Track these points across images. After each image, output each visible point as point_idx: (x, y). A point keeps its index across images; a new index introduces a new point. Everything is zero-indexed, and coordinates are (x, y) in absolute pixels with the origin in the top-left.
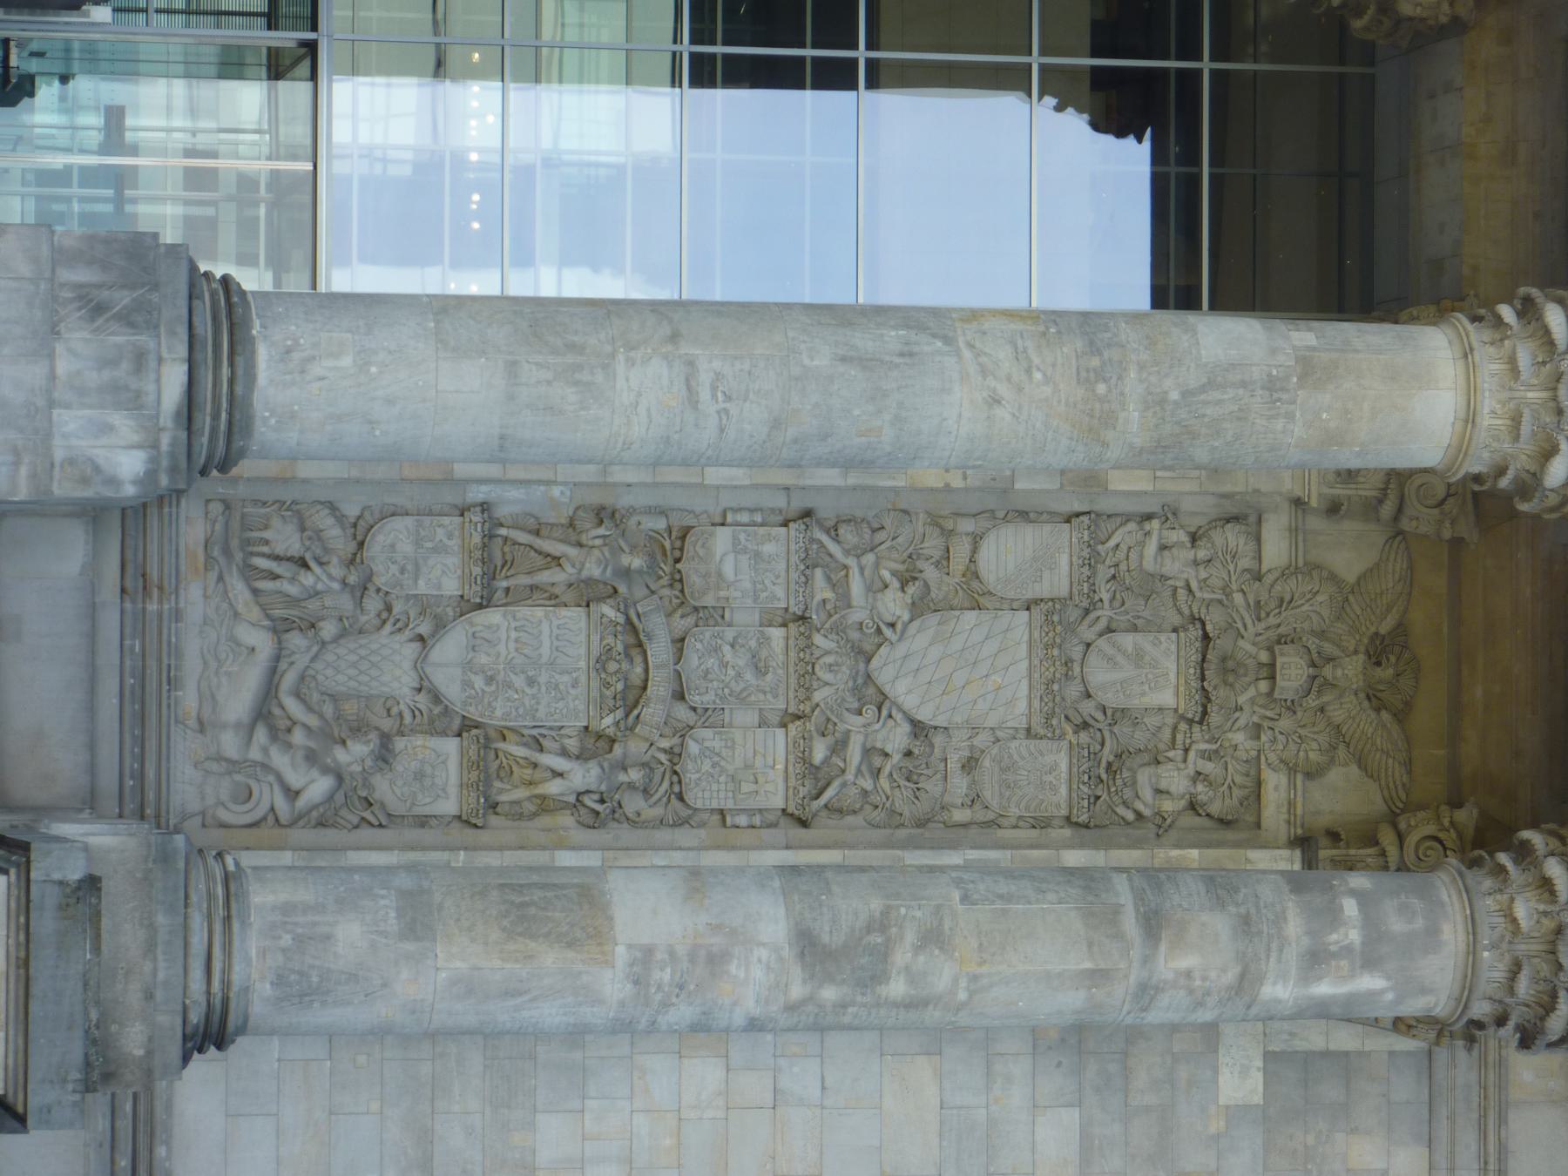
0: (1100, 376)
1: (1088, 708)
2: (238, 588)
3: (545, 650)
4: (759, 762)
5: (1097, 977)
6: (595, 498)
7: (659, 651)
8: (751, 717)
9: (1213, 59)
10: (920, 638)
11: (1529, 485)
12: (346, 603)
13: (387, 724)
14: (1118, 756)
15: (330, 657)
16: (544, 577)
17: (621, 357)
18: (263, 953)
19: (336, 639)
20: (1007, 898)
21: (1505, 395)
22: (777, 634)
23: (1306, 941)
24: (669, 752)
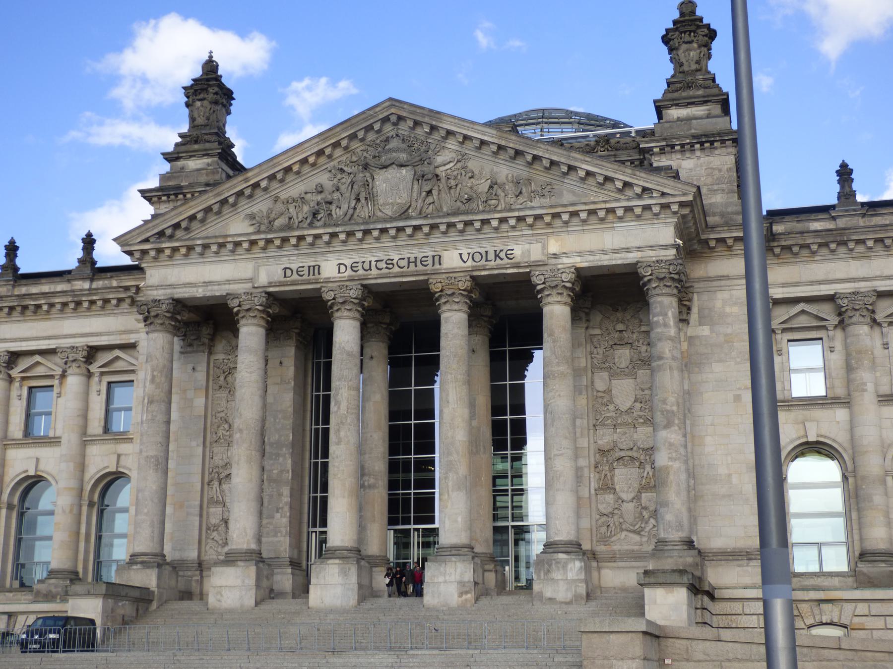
0: (554, 375)
1: (630, 367)
2: (614, 539)
3: (624, 477)
4: (644, 433)
5: (671, 368)
6: (592, 469)
7: (622, 454)
8: (635, 434)
9: (506, 347)
10: (617, 401)
11: (572, 289)
12: (616, 517)
13: (640, 507)
14: (640, 360)
15: (627, 520)
16: (609, 478)
17: (554, 469)
18: (673, 534)
19: (623, 519)
20: (656, 387)
21: (554, 296)
22: (618, 430)
23: (662, 327)
24: (643, 451)
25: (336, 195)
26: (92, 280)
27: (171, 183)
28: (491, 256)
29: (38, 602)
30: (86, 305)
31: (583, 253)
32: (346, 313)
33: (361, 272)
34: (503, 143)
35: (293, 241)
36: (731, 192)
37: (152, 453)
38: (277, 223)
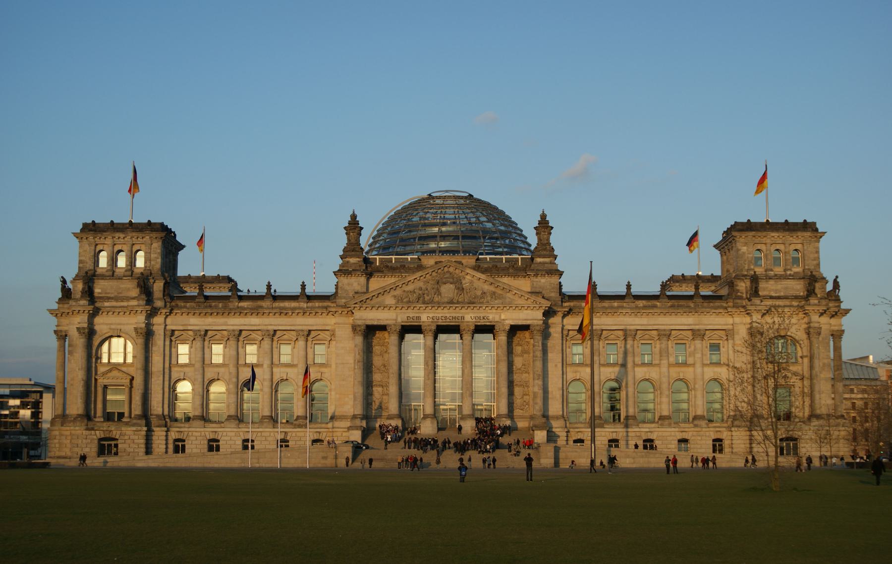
7: (518, 383)
10: (517, 365)
25: (426, 292)
26: (307, 303)
27: (344, 268)
28: (482, 318)
29: (296, 428)
30: (308, 314)
31: (513, 319)
32: (430, 334)
33: (436, 320)
34: (488, 280)
35: (412, 308)
36: (557, 292)
37: (360, 380)
38: (405, 300)
